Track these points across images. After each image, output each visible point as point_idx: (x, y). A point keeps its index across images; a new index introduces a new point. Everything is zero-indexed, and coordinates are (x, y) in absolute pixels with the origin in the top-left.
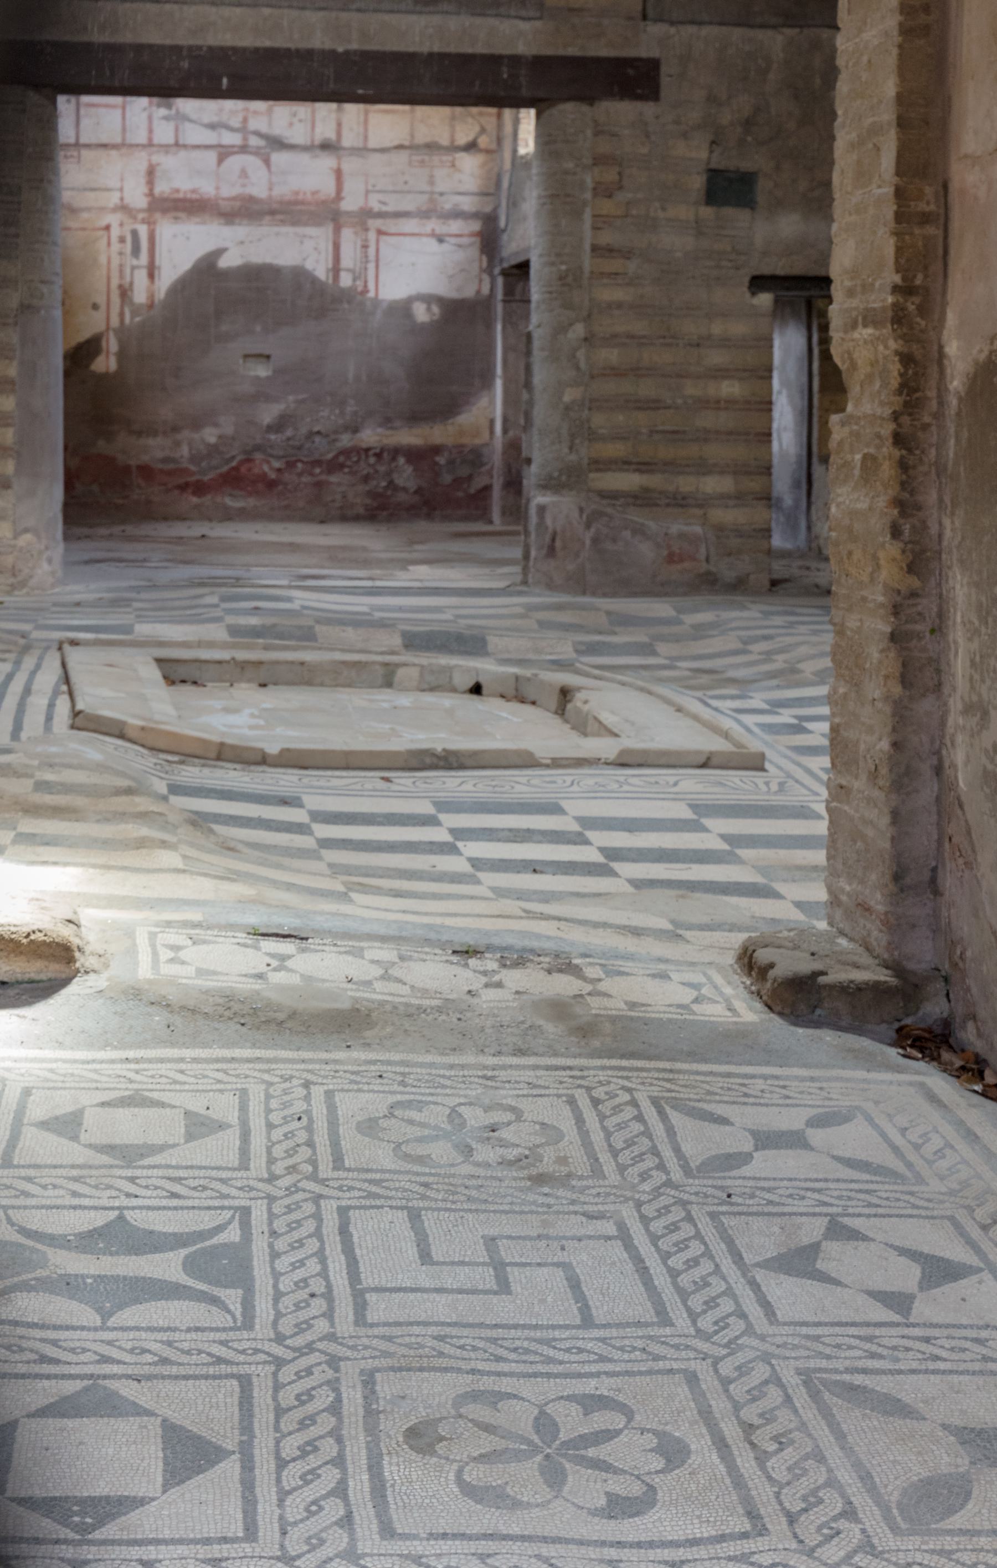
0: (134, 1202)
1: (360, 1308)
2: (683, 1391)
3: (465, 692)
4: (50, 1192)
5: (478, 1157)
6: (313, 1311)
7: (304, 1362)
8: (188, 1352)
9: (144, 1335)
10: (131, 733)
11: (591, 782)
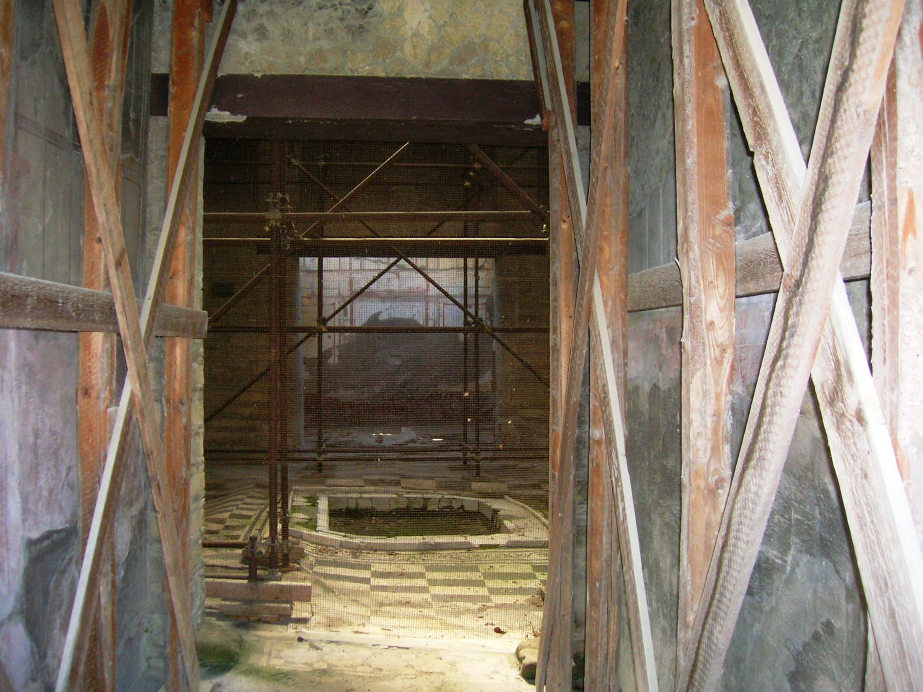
11: (493, 555)
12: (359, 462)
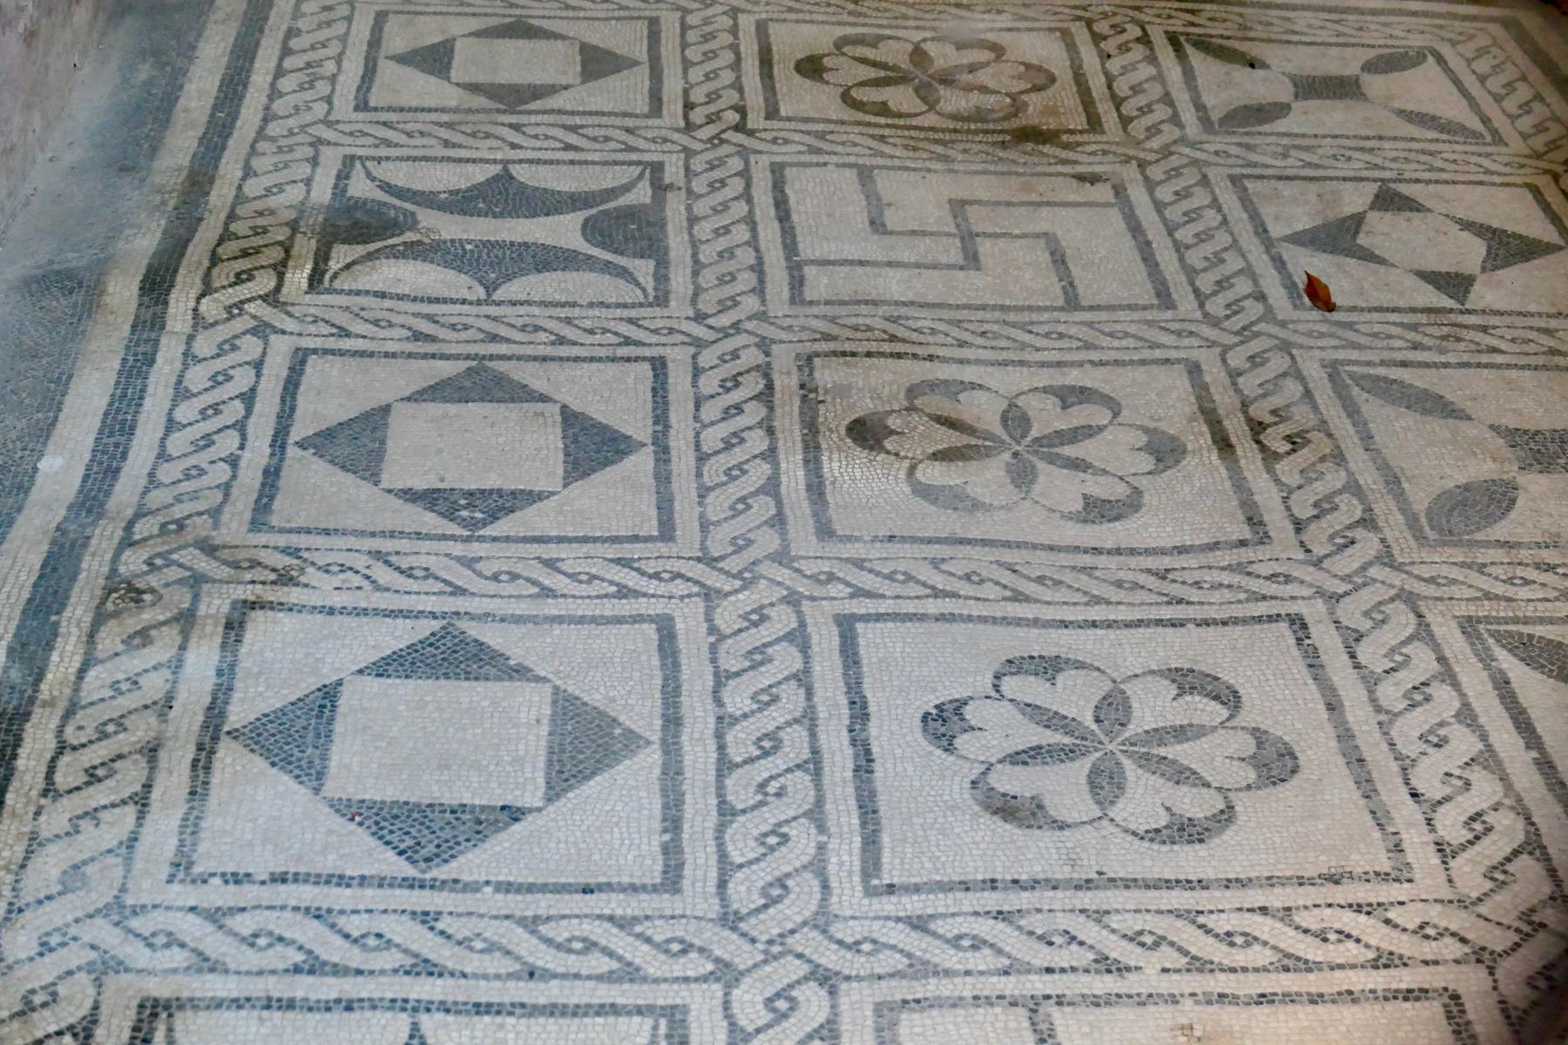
0: (520, 154)
2: (1183, 383)
4: (419, 141)
6: (740, 286)
7: (728, 345)
8: (591, 332)
9: (536, 310)
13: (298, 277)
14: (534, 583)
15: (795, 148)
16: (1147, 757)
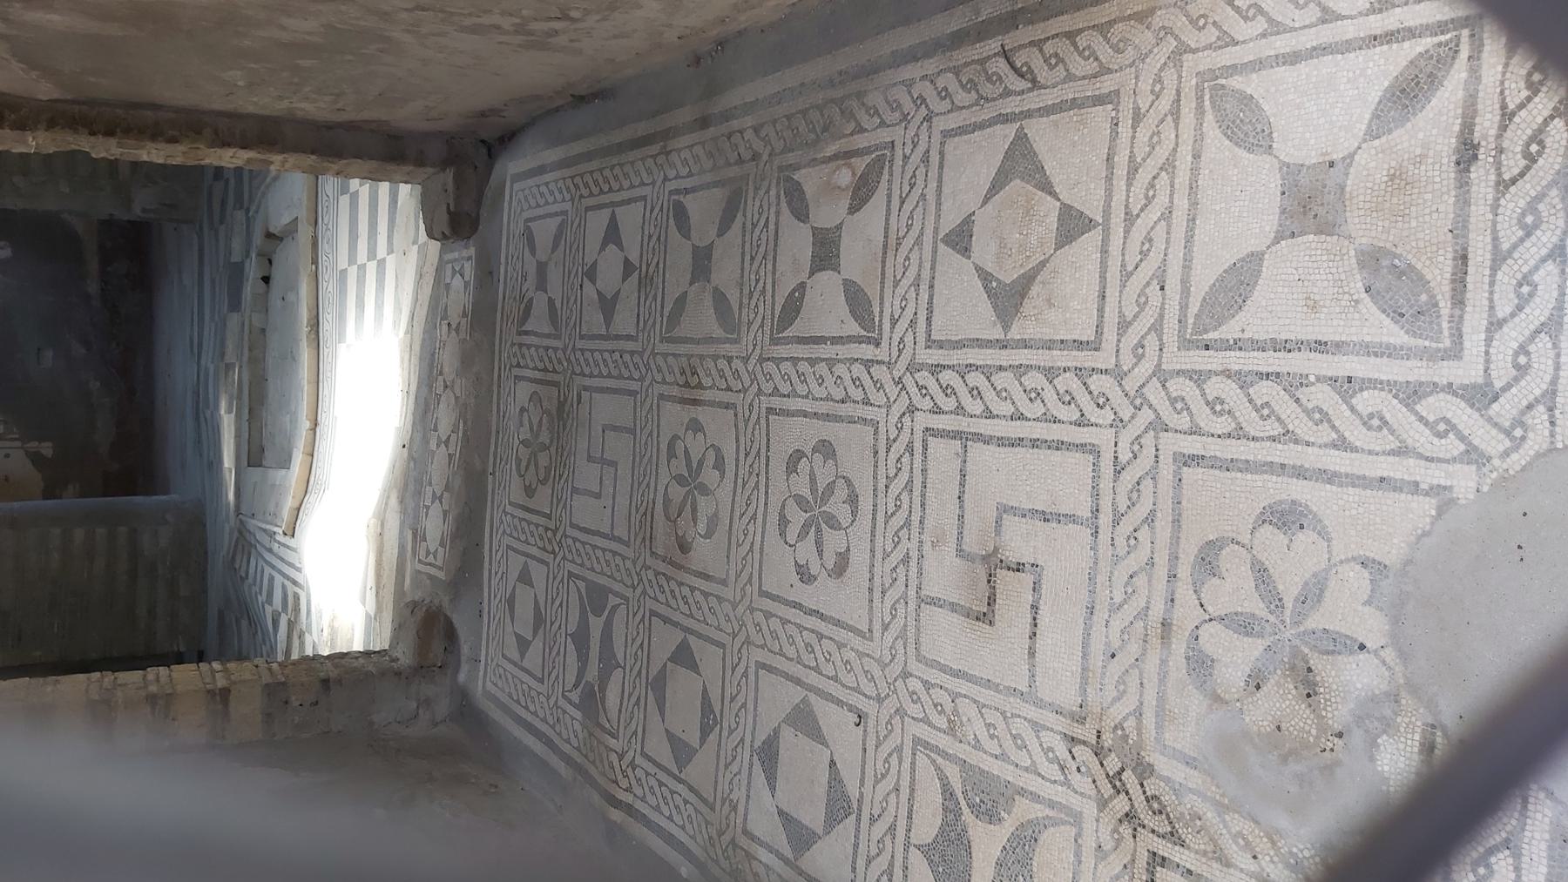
1: (619, 540)
3: (268, 287)
5: (547, 442)
10: (297, 505)
11: (326, 246)
12: (202, 419)
13: (612, 742)
14: (739, 710)
15: (563, 514)
16: (822, 500)
